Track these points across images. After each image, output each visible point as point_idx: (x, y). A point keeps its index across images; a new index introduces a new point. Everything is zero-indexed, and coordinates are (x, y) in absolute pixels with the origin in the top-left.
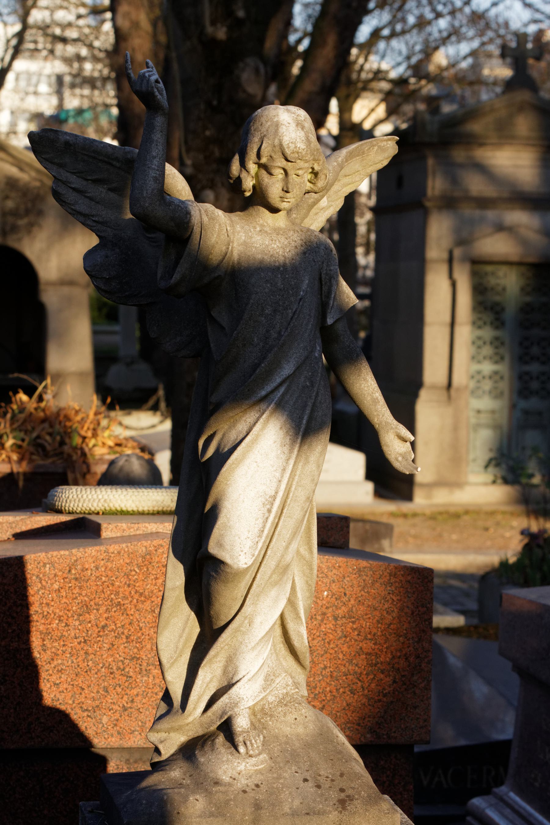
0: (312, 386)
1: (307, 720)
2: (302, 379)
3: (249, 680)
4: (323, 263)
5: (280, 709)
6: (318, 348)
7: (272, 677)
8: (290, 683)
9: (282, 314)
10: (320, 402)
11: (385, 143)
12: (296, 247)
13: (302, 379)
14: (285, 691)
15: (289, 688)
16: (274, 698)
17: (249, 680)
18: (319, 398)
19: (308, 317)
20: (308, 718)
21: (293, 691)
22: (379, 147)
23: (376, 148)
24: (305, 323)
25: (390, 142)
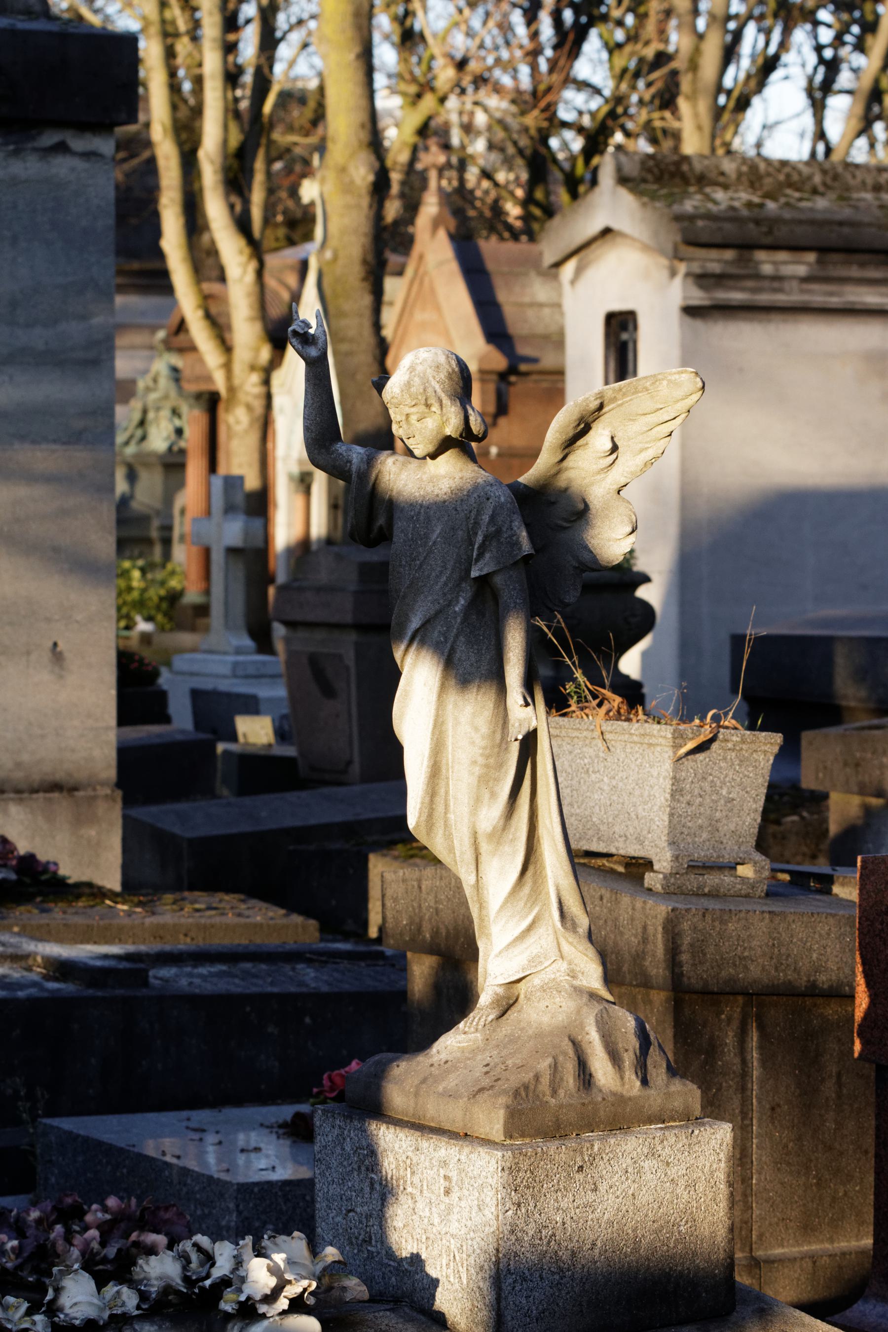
0: (446, 641)
1: (560, 1010)
2: (436, 634)
3: (497, 956)
4: (471, 512)
5: (539, 994)
6: (462, 602)
7: (542, 959)
8: (562, 969)
9: (410, 565)
10: (459, 660)
11: (677, 376)
12: (437, 495)
13: (436, 634)
14: (553, 976)
15: (558, 975)
16: (539, 982)
17: (497, 956)
18: (458, 655)
19: (439, 569)
20: (563, 1009)
21: (562, 978)
22: (670, 381)
23: (665, 383)
24: (434, 574)
25: (684, 375)
